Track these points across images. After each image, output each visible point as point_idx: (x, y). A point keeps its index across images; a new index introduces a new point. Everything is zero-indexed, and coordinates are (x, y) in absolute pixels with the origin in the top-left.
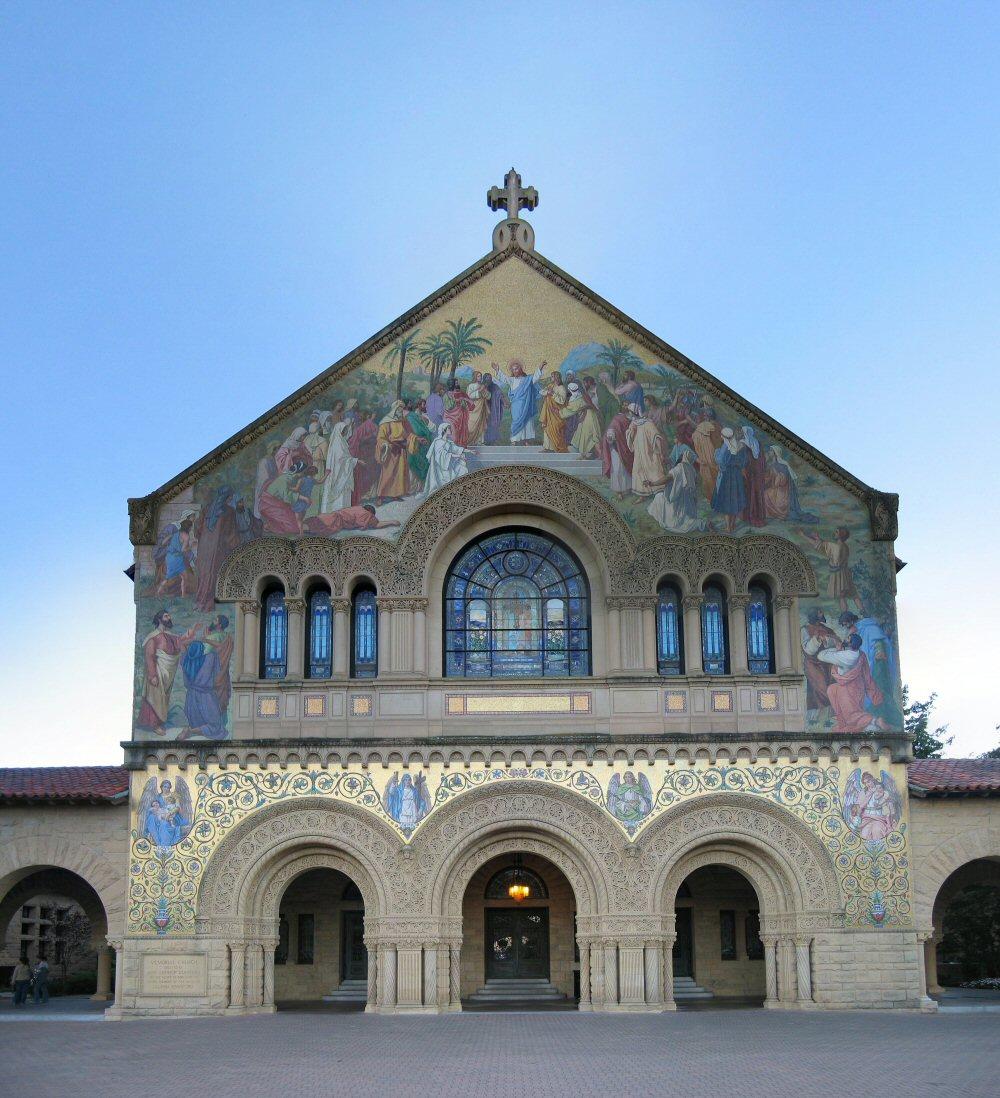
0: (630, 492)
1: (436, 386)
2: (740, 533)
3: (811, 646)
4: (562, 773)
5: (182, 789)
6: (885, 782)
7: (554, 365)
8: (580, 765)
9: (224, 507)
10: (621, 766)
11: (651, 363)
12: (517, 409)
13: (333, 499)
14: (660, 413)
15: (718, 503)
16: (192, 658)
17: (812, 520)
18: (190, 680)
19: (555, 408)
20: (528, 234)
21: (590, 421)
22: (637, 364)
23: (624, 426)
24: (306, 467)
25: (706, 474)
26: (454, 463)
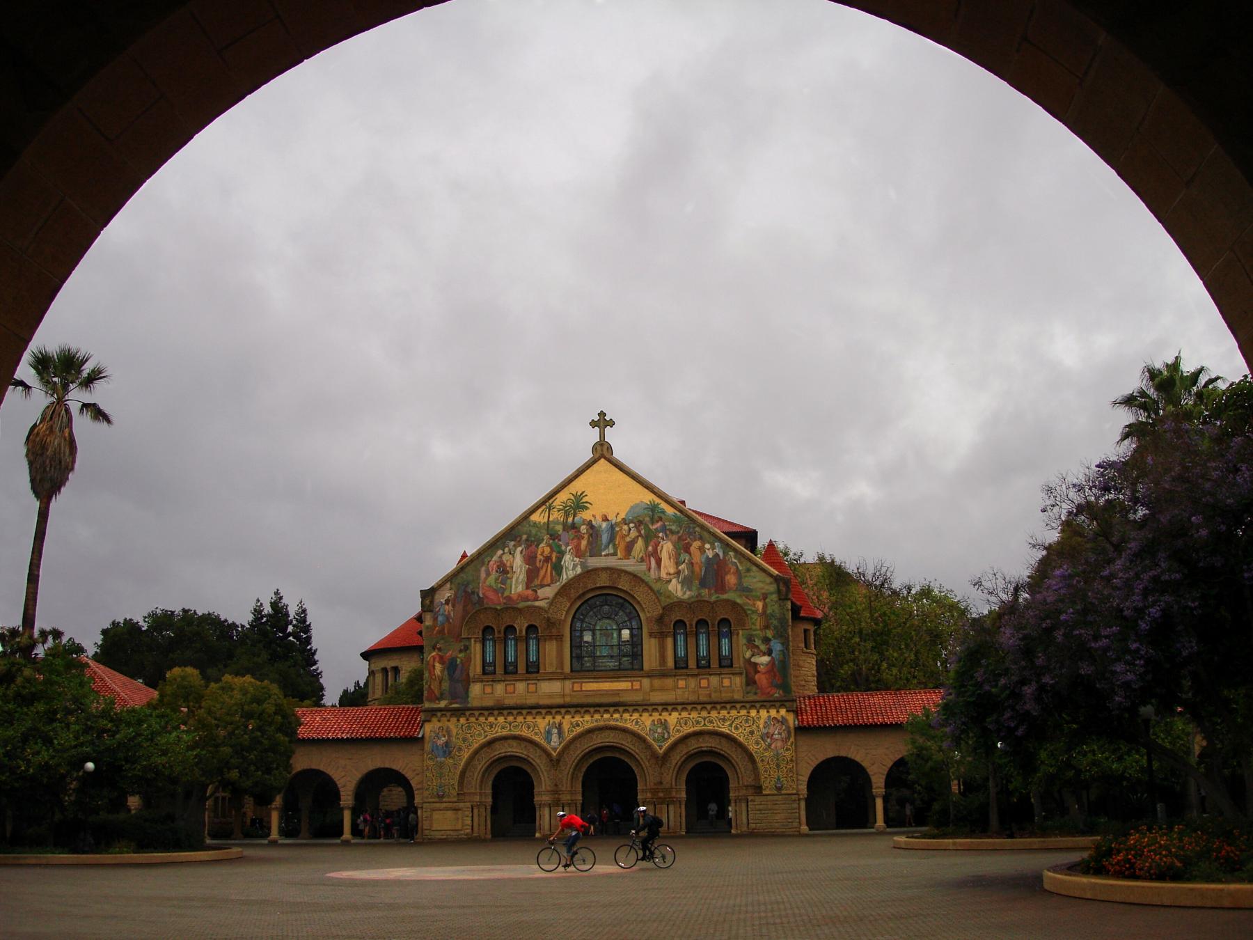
0: (659, 579)
1: (566, 527)
2: (713, 598)
3: (748, 654)
4: (628, 720)
5: (449, 732)
6: (783, 721)
7: (622, 515)
8: (636, 715)
9: (465, 592)
10: (656, 716)
11: (670, 511)
12: (605, 538)
13: (517, 586)
14: (675, 538)
15: (703, 584)
16: (451, 666)
17: (749, 590)
18: (451, 677)
19: (624, 537)
20: (610, 448)
21: (640, 542)
22: (663, 512)
23: (657, 545)
24: (504, 570)
25: (697, 569)
26: (575, 566)
